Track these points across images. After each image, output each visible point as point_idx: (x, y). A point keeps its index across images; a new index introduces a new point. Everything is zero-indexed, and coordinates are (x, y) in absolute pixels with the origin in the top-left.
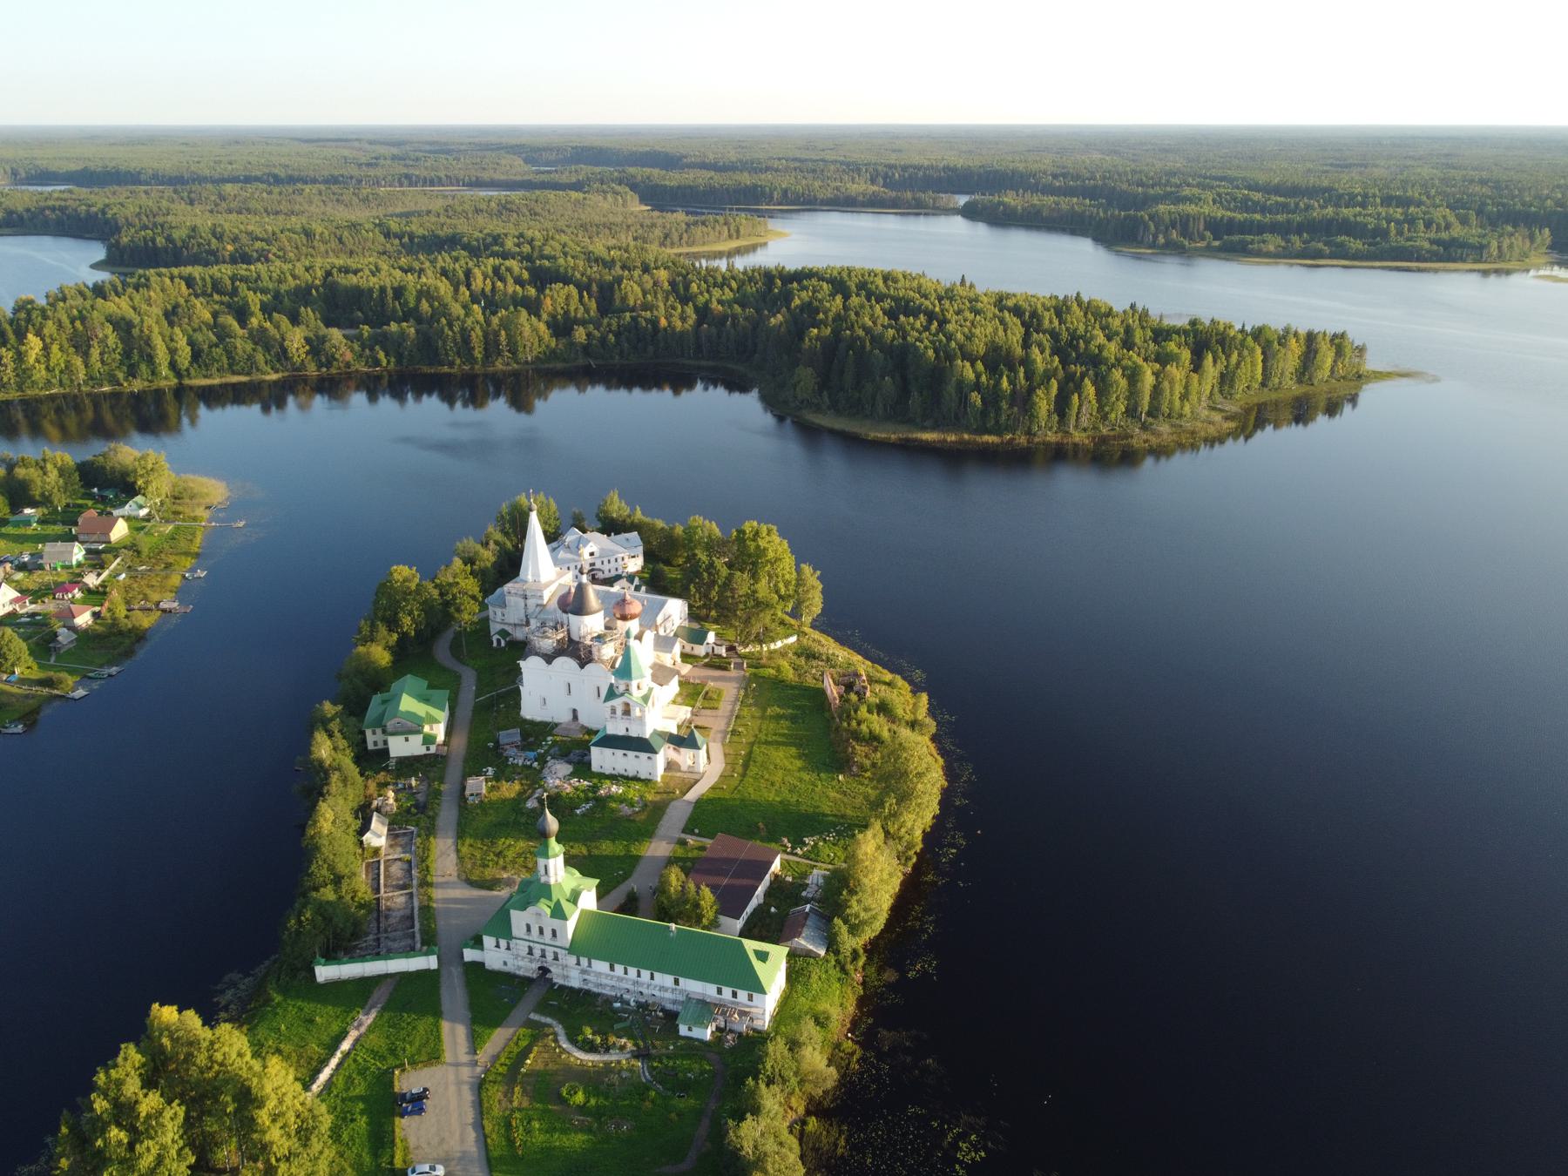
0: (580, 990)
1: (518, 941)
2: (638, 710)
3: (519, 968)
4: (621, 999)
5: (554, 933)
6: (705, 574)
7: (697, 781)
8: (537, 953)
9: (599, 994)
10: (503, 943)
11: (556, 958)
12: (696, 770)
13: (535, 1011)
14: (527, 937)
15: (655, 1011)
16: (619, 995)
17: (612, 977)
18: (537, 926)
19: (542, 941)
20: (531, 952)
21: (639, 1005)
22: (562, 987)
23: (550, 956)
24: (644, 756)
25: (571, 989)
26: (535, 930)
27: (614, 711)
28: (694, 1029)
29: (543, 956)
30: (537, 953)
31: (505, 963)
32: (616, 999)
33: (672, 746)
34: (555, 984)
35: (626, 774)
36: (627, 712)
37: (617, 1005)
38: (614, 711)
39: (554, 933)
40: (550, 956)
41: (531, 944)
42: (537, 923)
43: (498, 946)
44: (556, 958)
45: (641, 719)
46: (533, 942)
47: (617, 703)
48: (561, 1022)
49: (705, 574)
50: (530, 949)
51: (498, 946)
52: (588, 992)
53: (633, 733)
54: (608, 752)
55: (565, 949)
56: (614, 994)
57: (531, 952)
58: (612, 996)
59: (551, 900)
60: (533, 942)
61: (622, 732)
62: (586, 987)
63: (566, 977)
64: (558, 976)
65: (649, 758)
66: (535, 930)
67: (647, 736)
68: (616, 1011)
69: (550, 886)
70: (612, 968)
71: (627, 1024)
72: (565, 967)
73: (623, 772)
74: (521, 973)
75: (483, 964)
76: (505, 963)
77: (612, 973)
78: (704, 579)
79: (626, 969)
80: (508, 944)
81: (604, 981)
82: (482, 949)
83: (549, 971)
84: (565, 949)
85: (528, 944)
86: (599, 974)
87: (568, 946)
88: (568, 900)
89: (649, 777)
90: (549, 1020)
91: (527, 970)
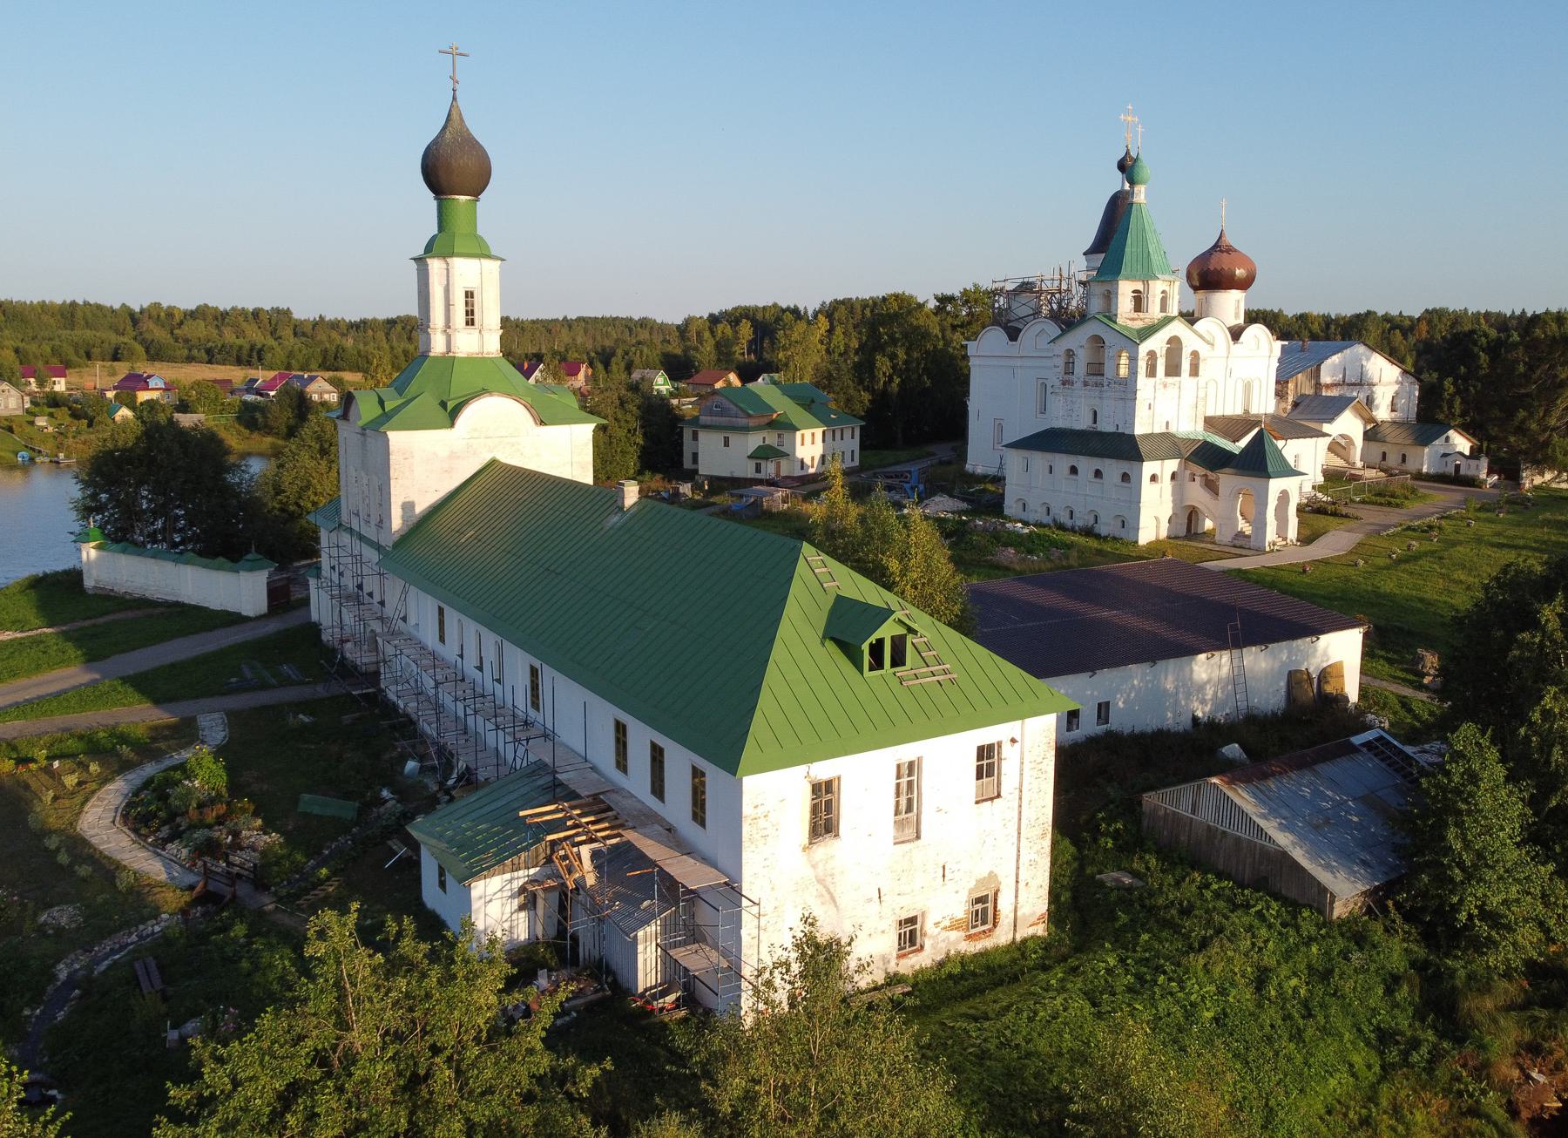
2: (1124, 361)
6: (1484, 358)
12: (1253, 543)
24: (1112, 468)
27: (1069, 367)
33: (1200, 471)
35: (1069, 523)
36: (1096, 369)
38: (1069, 367)
45: (1127, 391)
47: (1078, 339)
49: (1484, 358)
53: (1106, 426)
54: (1039, 460)
61: (1083, 423)
65: (1125, 477)
67: (1140, 429)
73: (1064, 518)
78: (1480, 367)
89: (1119, 532)
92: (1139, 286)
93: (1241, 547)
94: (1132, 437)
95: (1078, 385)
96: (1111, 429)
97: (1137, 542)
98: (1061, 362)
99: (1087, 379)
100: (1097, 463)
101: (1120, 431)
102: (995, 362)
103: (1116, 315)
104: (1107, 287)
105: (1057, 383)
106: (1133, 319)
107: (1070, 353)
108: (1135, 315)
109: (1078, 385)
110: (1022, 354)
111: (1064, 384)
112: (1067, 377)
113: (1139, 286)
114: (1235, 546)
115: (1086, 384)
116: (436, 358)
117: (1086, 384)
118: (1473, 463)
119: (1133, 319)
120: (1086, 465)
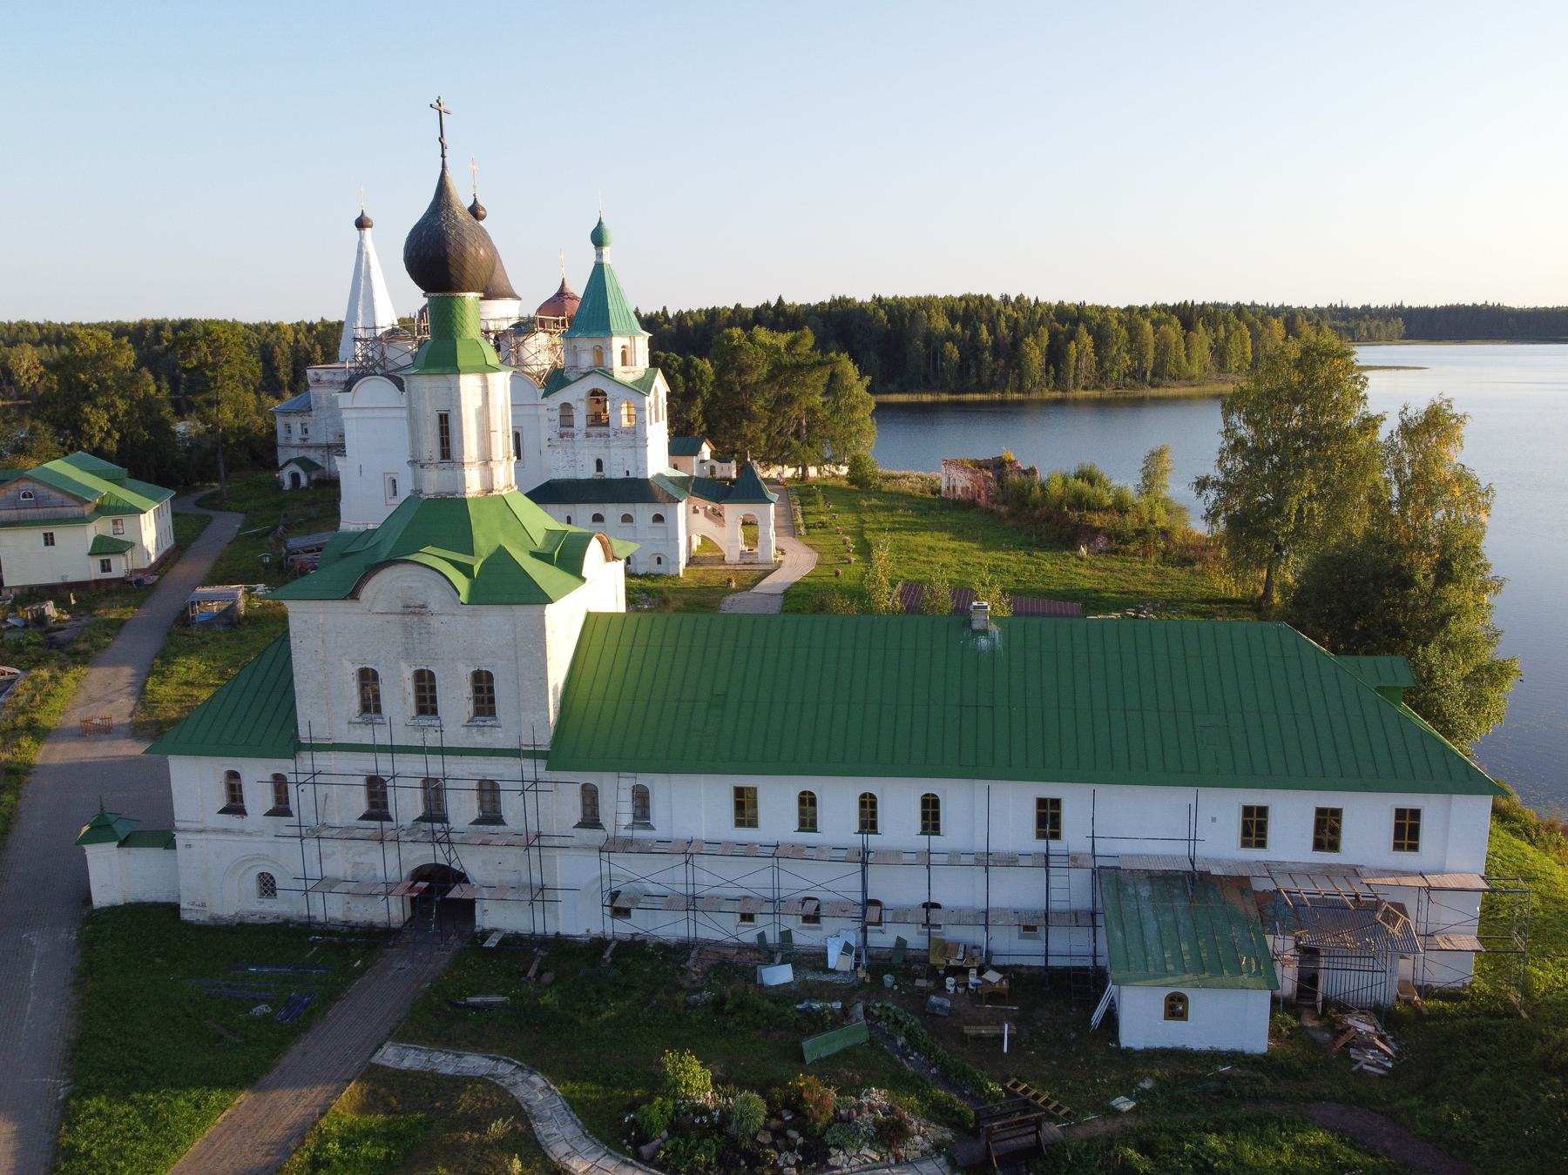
0: (599, 944)
1: (323, 761)
3: (326, 884)
4: (785, 951)
5: (483, 689)
7: (767, 573)
8: (407, 804)
9: (684, 948)
10: (257, 775)
11: (491, 816)
13: (402, 1035)
14: (363, 735)
15: (960, 972)
16: (772, 938)
17: (748, 851)
18: (408, 673)
19: (432, 740)
20: (378, 808)
21: (877, 964)
22: (515, 944)
23: (462, 808)
24: (643, 513)
25: (560, 947)
26: (398, 696)
28: (1200, 1001)
29: (435, 813)
30: (407, 804)
31: (267, 886)
32: (766, 953)
34: (486, 934)
36: (598, 421)
37: (780, 975)
39: (483, 689)
40: (462, 808)
41: (384, 764)
42: (408, 654)
43: (235, 806)
44: (491, 816)
46: (392, 749)
47: (576, 394)
48: (534, 1062)
50: (376, 787)
51: (235, 806)
52: (633, 948)
53: (614, 472)
55: (534, 755)
56: (748, 935)
57: (378, 808)
58: (743, 948)
59: (469, 550)
60: (392, 749)
61: (588, 472)
62: (623, 929)
63: (539, 894)
64: (500, 893)
66: (398, 696)
67: (649, 477)
68: (781, 995)
69: (464, 501)
70: (745, 808)
71: (855, 1033)
72: (534, 842)
74: (333, 909)
75: (173, 909)
76: (267, 886)
77: (745, 834)
79: (807, 801)
80: (279, 782)
81: (711, 877)
82: (169, 843)
83: (462, 878)
84: (534, 755)
85: (366, 763)
86: (689, 851)
87: (544, 739)
88: (535, 555)
90: (475, 1063)
91: (361, 890)
92: (626, 341)
93: (751, 563)
94: (647, 480)
95: (580, 437)
96: (621, 475)
97: (678, 575)
98: (556, 415)
99: (590, 430)
100: (627, 508)
101: (631, 476)
102: (378, 413)
103: (612, 369)
104: (599, 343)
105: (555, 436)
106: (626, 373)
107: (566, 407)
108: (626, 368)
109: (580, 437)
110: (355, 405)
111: (562, 436)
112: (565, 430)
113: (626, 341)
114: (745, 564)
115: (588, 435)
116: (476, 499)
117: (588, 435)
118: (725, 465)
119: (626, 373)
120: (612, 512)
